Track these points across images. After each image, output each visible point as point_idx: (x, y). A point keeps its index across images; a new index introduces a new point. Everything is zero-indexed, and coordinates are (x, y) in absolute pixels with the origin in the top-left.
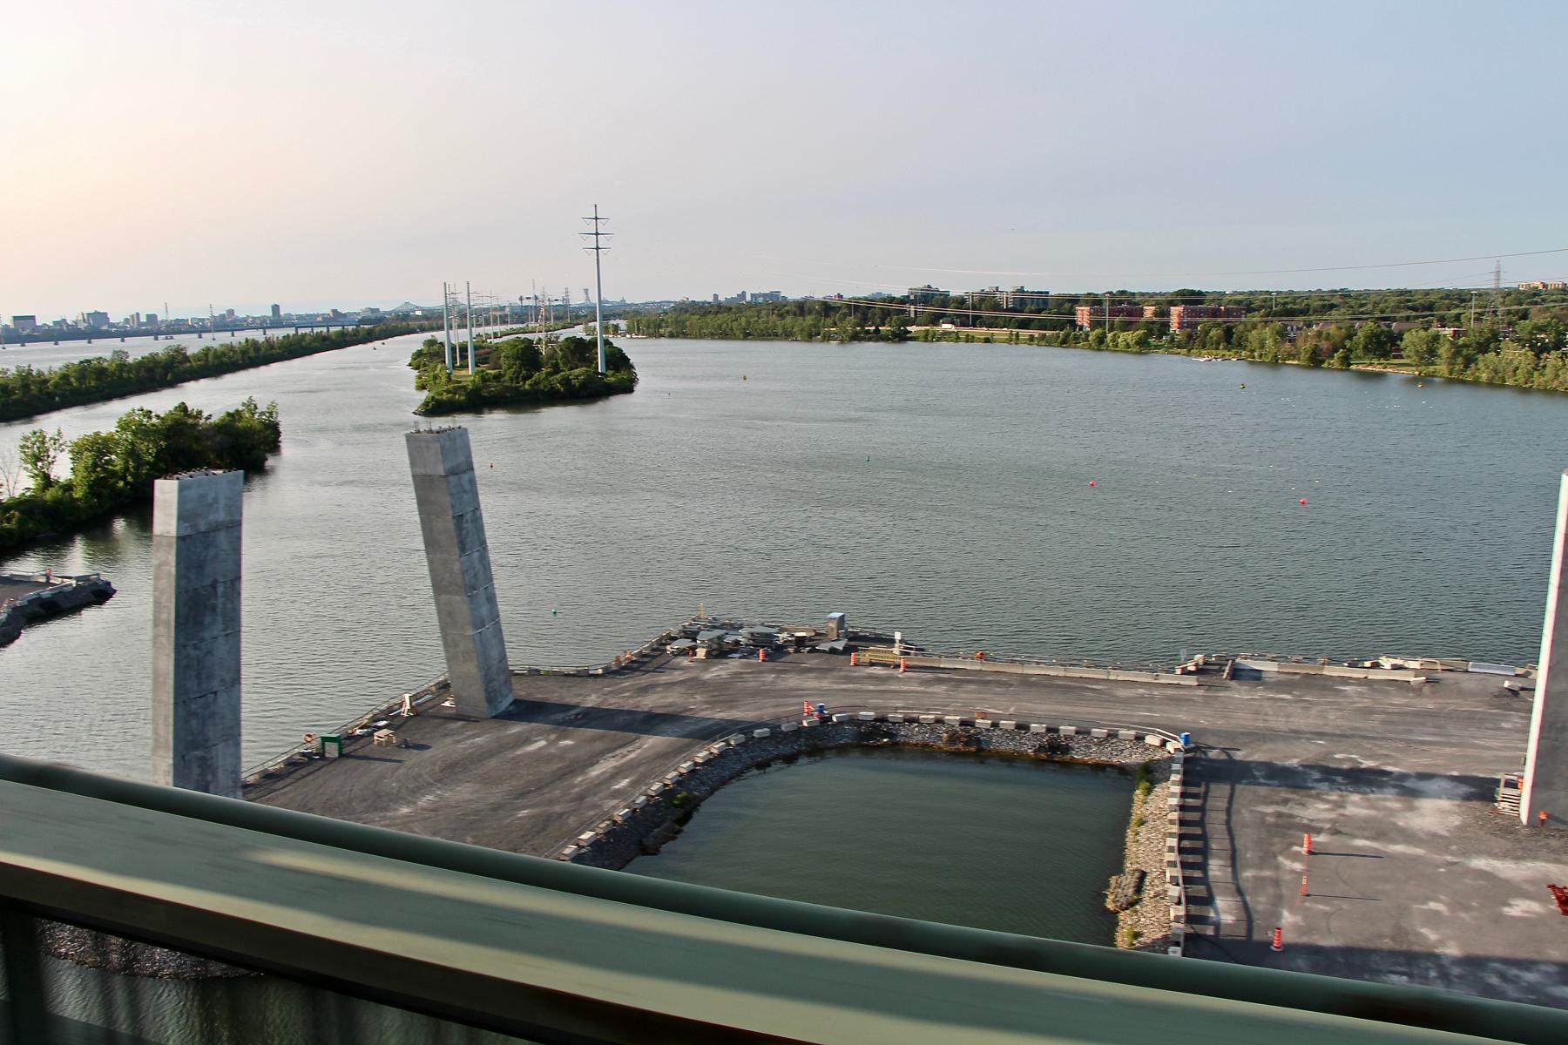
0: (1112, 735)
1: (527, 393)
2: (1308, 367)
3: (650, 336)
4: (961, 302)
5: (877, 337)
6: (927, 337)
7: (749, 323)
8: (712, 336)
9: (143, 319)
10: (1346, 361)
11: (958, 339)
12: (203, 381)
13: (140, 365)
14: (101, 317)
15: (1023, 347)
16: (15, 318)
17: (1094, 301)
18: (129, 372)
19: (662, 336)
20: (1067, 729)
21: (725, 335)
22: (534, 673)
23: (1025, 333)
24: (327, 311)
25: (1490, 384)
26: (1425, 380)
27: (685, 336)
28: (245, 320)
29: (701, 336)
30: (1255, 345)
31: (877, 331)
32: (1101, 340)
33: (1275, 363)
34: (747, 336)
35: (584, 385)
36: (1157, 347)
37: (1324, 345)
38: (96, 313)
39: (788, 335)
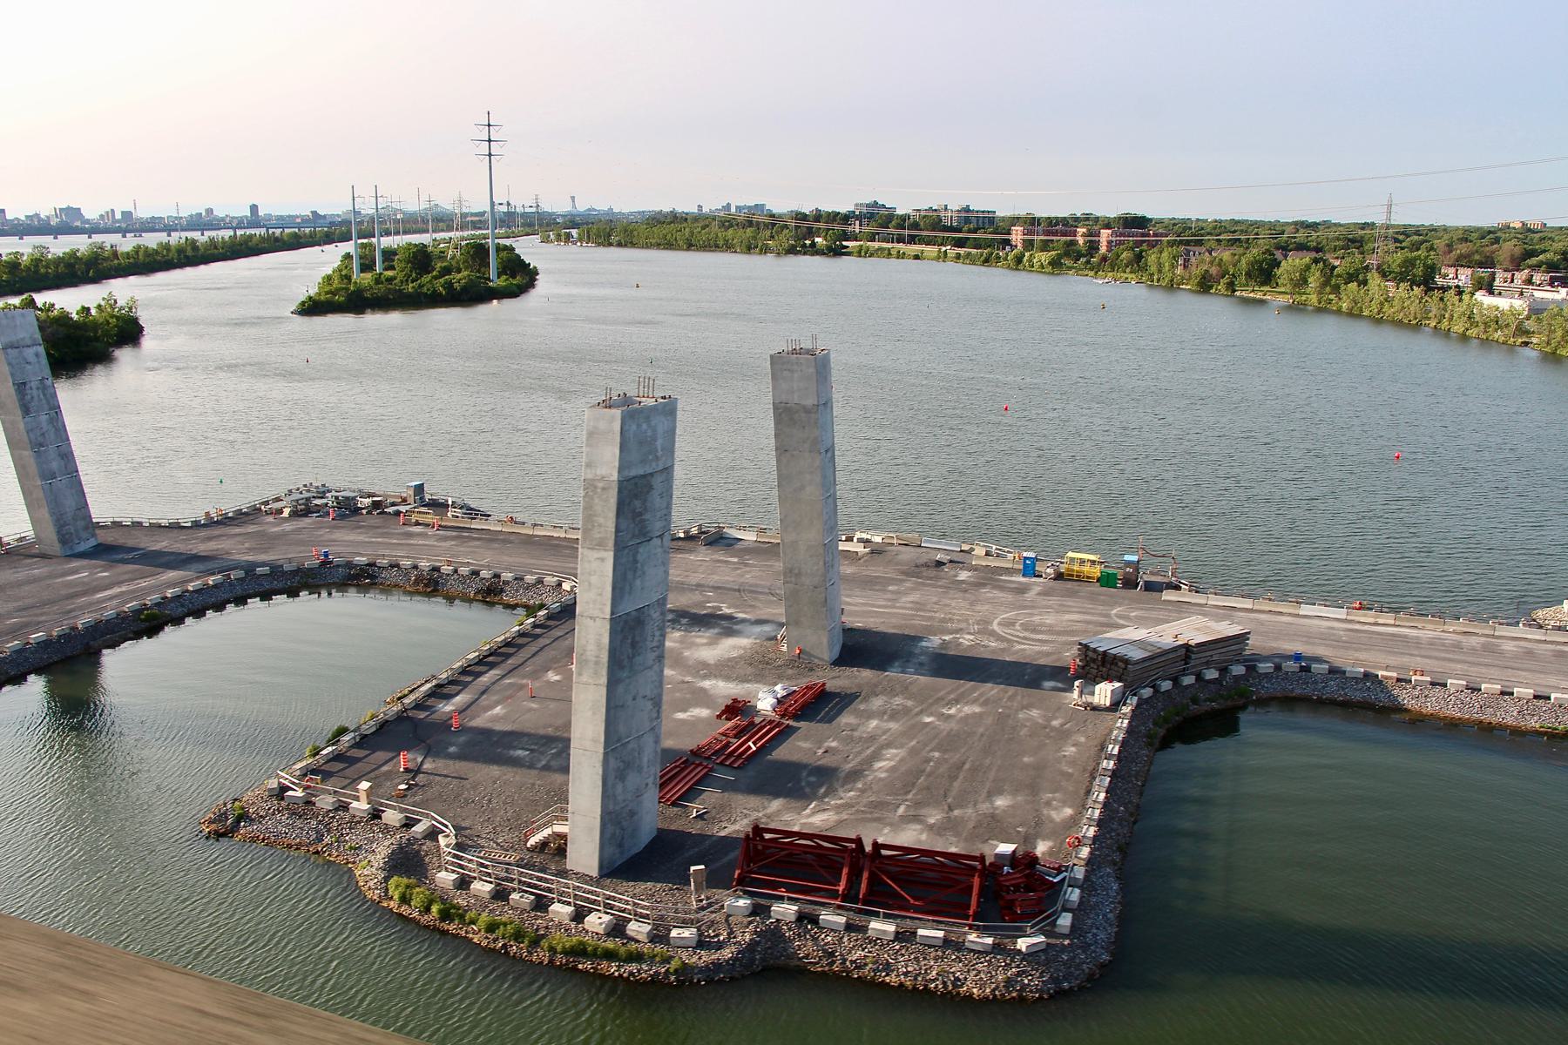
0: (540, 581)
1: (409, 295)
2: (1199, 292)
3: (599, 245)
4: (904, 218)
5: (814, 250)
6: (860, 253)
7: (692, 233)
8: (658, 246)
9: (118, 216)
10: (1231, 286)
11: (890, 255)
12: (132, 278)
13: (58, 261)
17: (1031, 222)
18: (47, 267)
19: (610, 245)
20: (507, 576)
21: (669, 245)
22: (117, 525)
24: (307, 212)
25: (1350, 314)
26: (1297, 308)
27: (633, 245)
28: (223, 219)
29: (648, 246)
30: (1153, 269)
31: (813, 244)
32: (1019, 260)
33: (1172, 287)
34: (690, 246)
35: (465, 289)
36: (1070, 268)
37: (1214, 270)
38: (69, 209)
39: (728, 247)
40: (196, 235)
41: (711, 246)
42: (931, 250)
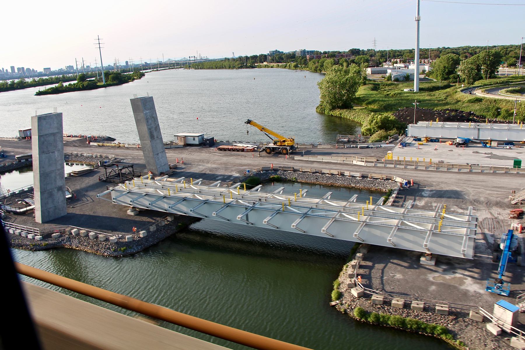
3: (196, 69)
5: (247, 67)
8: (209, 68)
9: (85, 67)
15: (280, 69)
23: (280, 64)
27: (204, 69)
35: (87, 86)
38: (70, 66)
41: (222, 67)
42: (276, 64)
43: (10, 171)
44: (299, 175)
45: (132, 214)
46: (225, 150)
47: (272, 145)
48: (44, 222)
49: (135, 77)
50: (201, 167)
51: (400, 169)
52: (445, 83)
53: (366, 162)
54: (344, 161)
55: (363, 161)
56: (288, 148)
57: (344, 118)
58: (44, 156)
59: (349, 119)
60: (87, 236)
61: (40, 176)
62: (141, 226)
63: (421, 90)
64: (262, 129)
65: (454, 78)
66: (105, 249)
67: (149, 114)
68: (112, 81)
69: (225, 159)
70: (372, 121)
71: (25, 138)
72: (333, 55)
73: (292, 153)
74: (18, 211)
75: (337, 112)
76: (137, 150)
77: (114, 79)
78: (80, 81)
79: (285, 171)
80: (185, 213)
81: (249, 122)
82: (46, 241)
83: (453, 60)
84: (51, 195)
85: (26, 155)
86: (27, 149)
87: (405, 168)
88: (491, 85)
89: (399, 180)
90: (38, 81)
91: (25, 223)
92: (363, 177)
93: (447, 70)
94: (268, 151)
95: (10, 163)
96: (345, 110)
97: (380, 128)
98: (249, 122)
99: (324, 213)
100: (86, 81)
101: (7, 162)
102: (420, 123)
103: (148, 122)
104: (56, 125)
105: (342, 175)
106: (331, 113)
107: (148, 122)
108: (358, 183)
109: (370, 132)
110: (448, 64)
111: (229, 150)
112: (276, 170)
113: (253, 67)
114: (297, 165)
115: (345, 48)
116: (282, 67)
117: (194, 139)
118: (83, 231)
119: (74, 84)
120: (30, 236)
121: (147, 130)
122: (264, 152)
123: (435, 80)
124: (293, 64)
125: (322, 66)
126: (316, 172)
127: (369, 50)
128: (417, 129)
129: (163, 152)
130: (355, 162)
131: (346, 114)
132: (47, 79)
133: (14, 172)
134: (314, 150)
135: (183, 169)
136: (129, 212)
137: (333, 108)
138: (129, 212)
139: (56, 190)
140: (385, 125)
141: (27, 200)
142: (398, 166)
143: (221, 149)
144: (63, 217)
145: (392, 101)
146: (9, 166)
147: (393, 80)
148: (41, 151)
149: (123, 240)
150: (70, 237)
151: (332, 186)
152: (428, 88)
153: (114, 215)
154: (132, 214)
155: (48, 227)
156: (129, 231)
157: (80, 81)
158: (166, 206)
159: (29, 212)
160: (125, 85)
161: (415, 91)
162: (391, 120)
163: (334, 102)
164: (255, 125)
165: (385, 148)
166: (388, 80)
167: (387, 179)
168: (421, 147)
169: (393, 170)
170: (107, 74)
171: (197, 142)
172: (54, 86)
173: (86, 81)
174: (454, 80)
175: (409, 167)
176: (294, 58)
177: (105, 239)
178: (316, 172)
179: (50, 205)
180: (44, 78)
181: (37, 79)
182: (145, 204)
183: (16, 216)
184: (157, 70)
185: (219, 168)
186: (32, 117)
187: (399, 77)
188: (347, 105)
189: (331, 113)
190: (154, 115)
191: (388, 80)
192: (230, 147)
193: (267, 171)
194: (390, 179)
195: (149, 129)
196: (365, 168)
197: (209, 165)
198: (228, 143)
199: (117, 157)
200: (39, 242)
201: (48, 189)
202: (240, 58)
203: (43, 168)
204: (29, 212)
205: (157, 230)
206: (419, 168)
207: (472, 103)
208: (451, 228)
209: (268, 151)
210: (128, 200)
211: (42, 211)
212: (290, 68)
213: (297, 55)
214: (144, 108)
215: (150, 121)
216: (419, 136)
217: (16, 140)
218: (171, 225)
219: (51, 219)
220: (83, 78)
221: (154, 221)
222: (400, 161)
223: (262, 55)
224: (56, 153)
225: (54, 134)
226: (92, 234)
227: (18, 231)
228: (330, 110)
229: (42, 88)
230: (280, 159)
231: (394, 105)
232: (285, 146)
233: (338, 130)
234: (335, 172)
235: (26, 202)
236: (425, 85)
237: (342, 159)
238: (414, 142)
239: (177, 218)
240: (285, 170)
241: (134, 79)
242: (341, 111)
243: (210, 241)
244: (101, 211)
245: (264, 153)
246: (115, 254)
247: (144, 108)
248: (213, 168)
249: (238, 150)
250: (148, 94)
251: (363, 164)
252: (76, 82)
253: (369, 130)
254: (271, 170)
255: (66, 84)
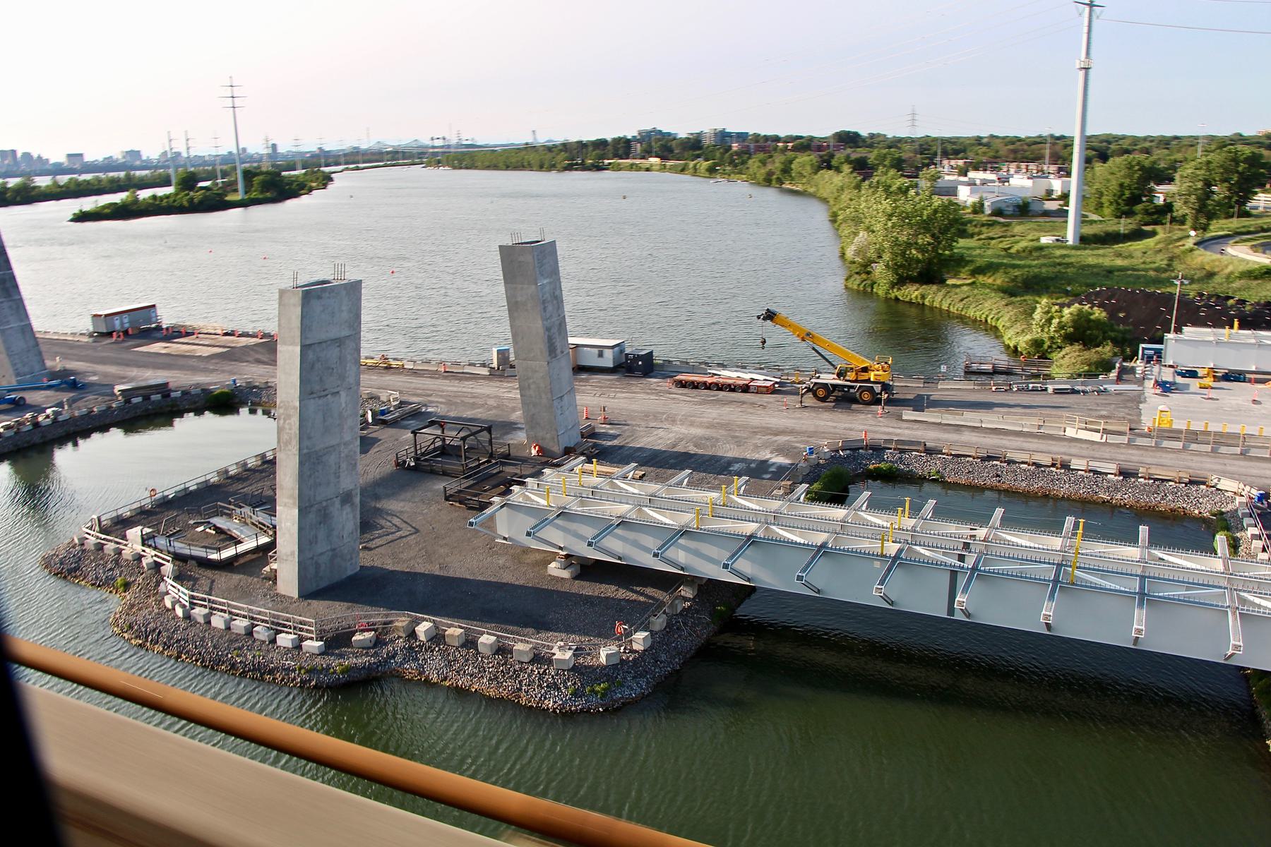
3: (454, 168)
8: (488, 168)
14: (135, 154)
15: (667, 175)
16: (69, 156)
21: (495, 167)
23: (669, 163)
24: (314, 149)
27: (476, 168)
28: (252, 156)
31: (583, 163)
35: (201, 202)
40: (101, 175)
43: (104, 428)
44: (945, 462)
45: (566, 574)
46: (694, 386)
47: (829, 378)
48: (309, 592)
49: (314, 184)
50: (661, 433)
51: (1200, 454)
52: (1124, 226)
53: (1106, 431)
54: (1040, 427)
55: (1098, 431)
56: (878, 388)
57: (932, 308)
58: (312, 404)
59: (941, 309)
60: (470, 643)
61: (301, 463)
62: (636, 615)
63: (1084, 240)
64: (807, 336)
65: (1147, 212)
66: (540, 686)
67: (547, 288)
68: (262, 192)
69: (713, 413)
70: (1049, 321)
71: (110, 334)
72: (804, 145)
73: (890, 402)
74: (214, 556)
75: (912, 292)
76: (445, 378)
77: (265, 186)
78: (182, 190)
79: (902, 451)
80: (620, 558)
81: (770, 316)
82: (341, 656)
83: (1142, 168)
84: (325, 516)
85: (143, 384)
86: (127, 365)
87: (1213, 450)
88: (1249, 233)
89: (1227, 484)
90: (66, 186)
91: (244, 594)
92: (1125, 474)
93: (1127, 194)
94: (821, 393)
95: (103, 407)
96: (935, 287)
97: (1070, 339)
98: (770, 316)
99: (1181, 592)
100: (198, 191)
101: (95, 404)
102: (1189, 331)
103: (545, 309)
104: (345, 315)
105: (1065, 466)
106: (895, 293)
107: (545, 309)
108: (1117, 490)
109: (1041, 351)
110: (1130, 176)
111: (708, 387)
112: (877, 450)
113: (599, 168)
114: (931, 437)
115: (823, 129)
116: (673, 170)
117: (601, 355)
118: (454, 631)
119: (167, 197)
120: (285, 640)
121: (541, 331)
122: (810, 395)
123: (1095, 217)
124: (705, 164)
125: (786, 170)
126: (989, 458)
127: (872, 136)
128: (1189, 345)
129: (572, 391)
130: (1070, 432)
131: (934, 297)
132: (88, 182)
133: (114, 430)
134: (936, 396)
135: (615, 437)
136: (554, 569)
137: (901, 281)
138: (554, 569)
139: (337, 502)
140: (1081, 334)
141: (220, 522)
142: (1193, 446)
143: (682, 385)
144: (353, 580)
145: (1035, 265)
146: (103, 414)
147: (988, 211)
148: (309, 389)
149: (589, 661)
150: (411, 648)
151: (1046, 496)
152: (1095, 236)
153: (507, 578)
154: (566, 574)
155: (336, 612)
156: (606, 633)
157: (182, 190)
158: (681, 557)
159: (242, 561)
160: (291, 203)
161: (1070, 242)
162: (1098, 321)
163: (902, 266)
164: (785, 324)
165: (1119, 394)
166: (975, 212)
167: (1191, 482)
168: (1213, 394)
169: (1183, 456)
170: (249, 175)
171: (608, 360)
172: (118, 198)
173: (198, 191)
174: (1147, 219)
175: (1223, 450)
176: (700, 148)
177: (531, 656)
178: (989, 458)
179: (322, 547)
180: (138, 173)
181: (63, 179)
182: (617, 548)
183: (209, 573)
184: (358, 169)
185: (717, 440)
186: (282, 293)
187: (1003, 206)
188: (931, 274)
189: (895, 293)
190: (557, 293)
191: (975, 212)
192: (710, 380)
193: (854, 449)
194: (1204, 483)
195: (548, 329)
196: (1103, 448)
197: (681, 430)
198: (687, 367)
199: (405, 398)
200: (321, 662)
201: (318, 499)
202: (565, 146)
203: (309, 438)
204: (242, 561)
205: (669, 625)
206: (1253, 453)
207: (1256, 278)
208: (1188, 589)
209: (821, 393)
210: (556, 536)
211: (300, 563)
212: (695, 172)
213: (707, 142)
214: (530, 269)
215: (550, 308)
216: (1190, 365)
217: (86, 339)
218: (697, 612)
219: (323, 584)
220: (188, 182)
221: (642, 599)
222: (1195, 433)
223: (620, 139)
224: (343, 394)
225: (339, 342)
226: (487, 640)
227: (240, 624)
228: (893, 285)
229: (89, 203)
230: (862, 416)
231: (1052, 279)
232: (868, 381)
233: (911, 333)
234: (1046, 460)
235: (216, 528)
236: (1088, 230)
237: (1035, 421)
238: (1179, 380)
239: (708, 588)
240: (903, 448)
241: (311, 190)
242: (924, 289)
243: (785, 650)
244: (465, 565)
245: (809, 400)
246: (580, 704)
247: (530, 269)
248: (701, 438)
249: (732, 388)
250: (542, 231)
251: (1096, 437)
252: (169, 190)
253: (1037, 344)
254: (866, 448)
255: (144, 194)
